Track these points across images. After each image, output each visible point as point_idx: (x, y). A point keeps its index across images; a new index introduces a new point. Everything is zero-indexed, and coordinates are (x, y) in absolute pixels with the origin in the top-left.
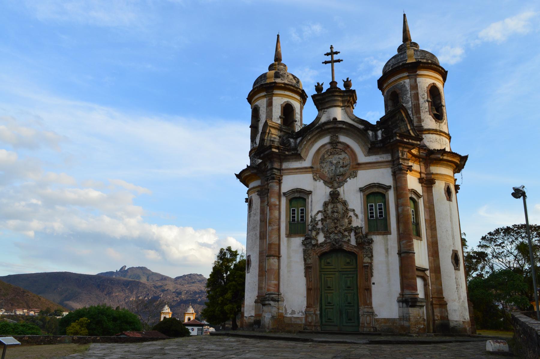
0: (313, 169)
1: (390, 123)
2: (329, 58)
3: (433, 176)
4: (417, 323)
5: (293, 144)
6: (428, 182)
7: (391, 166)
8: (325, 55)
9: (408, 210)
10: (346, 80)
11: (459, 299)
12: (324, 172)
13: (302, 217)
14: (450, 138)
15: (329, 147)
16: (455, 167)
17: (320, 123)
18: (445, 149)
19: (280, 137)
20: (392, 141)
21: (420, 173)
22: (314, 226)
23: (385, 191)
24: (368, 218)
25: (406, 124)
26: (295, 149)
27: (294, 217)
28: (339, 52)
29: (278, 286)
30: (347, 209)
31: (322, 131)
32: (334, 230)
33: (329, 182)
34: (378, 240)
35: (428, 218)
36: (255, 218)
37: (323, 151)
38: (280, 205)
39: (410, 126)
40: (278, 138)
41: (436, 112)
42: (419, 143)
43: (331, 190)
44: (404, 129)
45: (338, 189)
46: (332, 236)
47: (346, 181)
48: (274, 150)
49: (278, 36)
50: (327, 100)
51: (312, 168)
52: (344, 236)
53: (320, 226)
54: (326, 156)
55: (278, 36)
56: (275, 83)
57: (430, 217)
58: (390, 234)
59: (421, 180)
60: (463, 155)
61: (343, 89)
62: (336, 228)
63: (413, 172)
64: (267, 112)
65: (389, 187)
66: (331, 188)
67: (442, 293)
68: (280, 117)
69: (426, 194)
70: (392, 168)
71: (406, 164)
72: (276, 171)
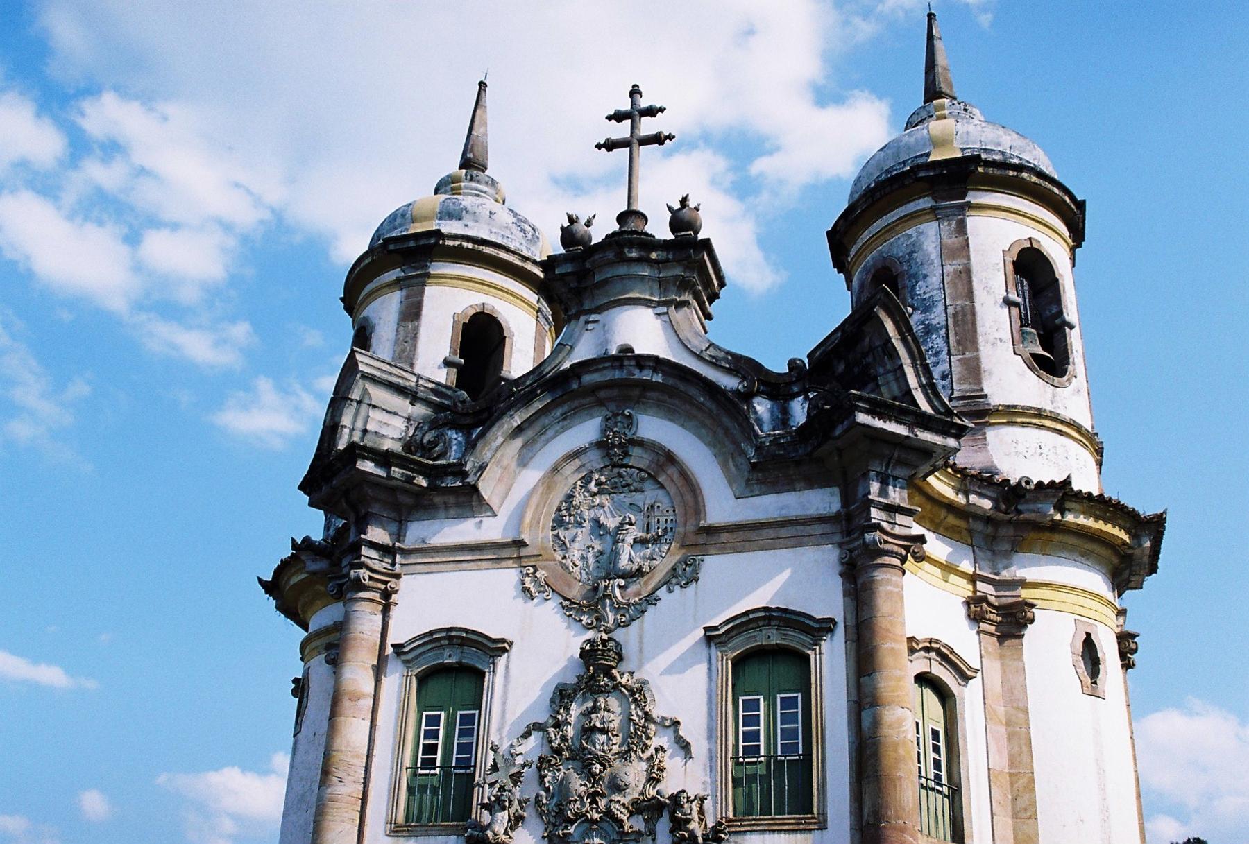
0: (524, 552)
1: (841, 367)
2: (622, 130)
3: (1025, 594)
7: (837, 538)
8: (609, 118)
9: (900, 722)
10: (677, 206)
12: (569, 562)
14: (1099, 451)
15: (595, 459)
16: (1115, 560)
18: (1067, 482)
20: (838, 431)
21: (973, 579)
22: (502, 789)
23: (808, 640)
24: (736, 757)
25: (901, 367)
27: (431, 749)
28: (662, 110)
30: (648, 717)
31: (574, 395)
35: (1001, 763)
39: (918, 376)
43: (590, 635)
44: (894, 386)
45: (619, 635)
47: (651, 599)
48: (368, 466)
49: (482, 85)
50: (597, 278)
54: (579, 499)
55: (482, 85)
56: (437, 234)
57: (1012, 764)
58: (822, 825)
59: (976, 609)
60: (1146, 509)
62: (593, 796)
63: (925, 564)
64: (396, 342)
65: (825, 627)
66: (588, 627)
68: (447, 363)
69: (997, 665)
70: (840, 545)
71: (897, 530)
72: (373, 554)
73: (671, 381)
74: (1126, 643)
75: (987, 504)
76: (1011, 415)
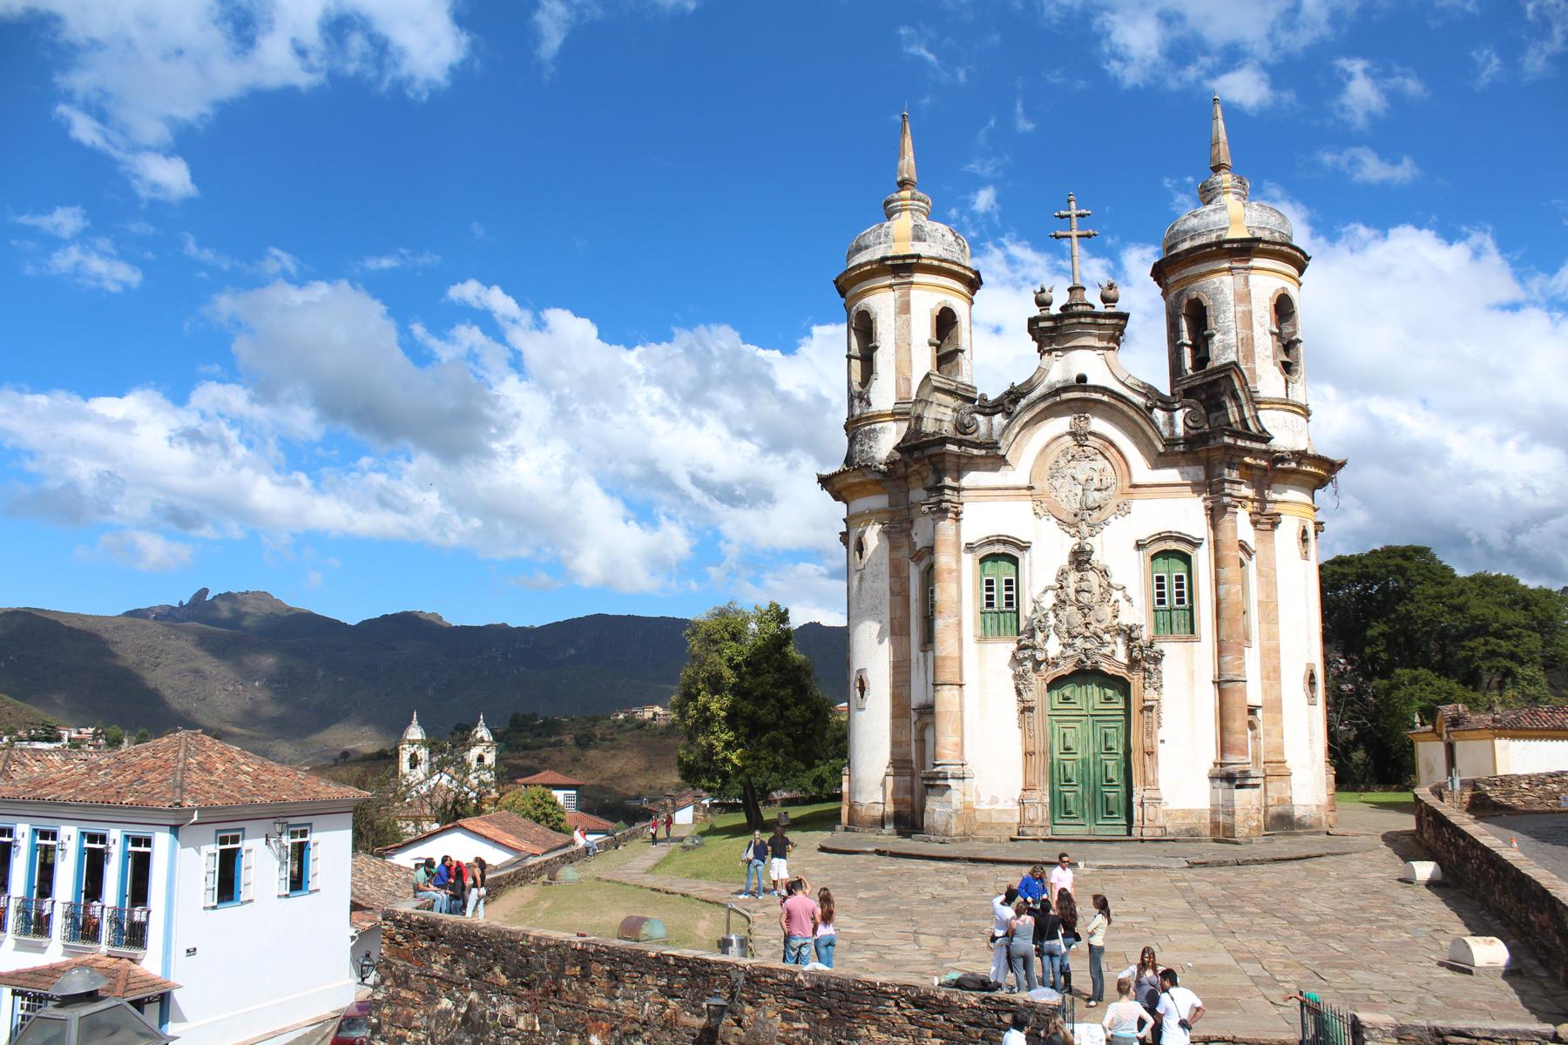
4: (1247, 818)
5: (983, 429)
6: (1267, 521)
10: (1105, 285)
11: (1313, 761)
13: (1009, 597)
17: (1046, 382)
19: (954, 410)
26: (992, 445)
27: (990, 597)
29: (961, 746)
30: (1109, 585)
32: (1083, 630)
33: (1071, 523)
34: (1174, 653)
36: (878, 585)
37: (1056, 449)
38: (959, 570)
40: (949, 411)
41: (1285, 359)
42: (1263, 447)
46: (1079, 642)
47: (1105, 522)
48: (951, 448)
51: (1030, 488)
52: (1103, 644)
53: (1052, 621)
54: (1062, 463)
56: (919, 257)
61: (1100, 307)
62: (1087, 625)
67: (1282, 753)
71: (1235, 493)
73: (1113, 401)
74: (1319, 525)
75: (1264, 463)
76: (1272, 403)
